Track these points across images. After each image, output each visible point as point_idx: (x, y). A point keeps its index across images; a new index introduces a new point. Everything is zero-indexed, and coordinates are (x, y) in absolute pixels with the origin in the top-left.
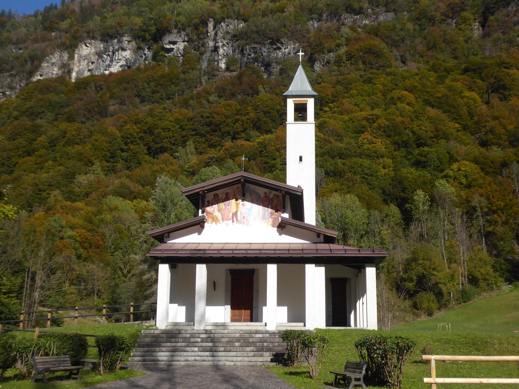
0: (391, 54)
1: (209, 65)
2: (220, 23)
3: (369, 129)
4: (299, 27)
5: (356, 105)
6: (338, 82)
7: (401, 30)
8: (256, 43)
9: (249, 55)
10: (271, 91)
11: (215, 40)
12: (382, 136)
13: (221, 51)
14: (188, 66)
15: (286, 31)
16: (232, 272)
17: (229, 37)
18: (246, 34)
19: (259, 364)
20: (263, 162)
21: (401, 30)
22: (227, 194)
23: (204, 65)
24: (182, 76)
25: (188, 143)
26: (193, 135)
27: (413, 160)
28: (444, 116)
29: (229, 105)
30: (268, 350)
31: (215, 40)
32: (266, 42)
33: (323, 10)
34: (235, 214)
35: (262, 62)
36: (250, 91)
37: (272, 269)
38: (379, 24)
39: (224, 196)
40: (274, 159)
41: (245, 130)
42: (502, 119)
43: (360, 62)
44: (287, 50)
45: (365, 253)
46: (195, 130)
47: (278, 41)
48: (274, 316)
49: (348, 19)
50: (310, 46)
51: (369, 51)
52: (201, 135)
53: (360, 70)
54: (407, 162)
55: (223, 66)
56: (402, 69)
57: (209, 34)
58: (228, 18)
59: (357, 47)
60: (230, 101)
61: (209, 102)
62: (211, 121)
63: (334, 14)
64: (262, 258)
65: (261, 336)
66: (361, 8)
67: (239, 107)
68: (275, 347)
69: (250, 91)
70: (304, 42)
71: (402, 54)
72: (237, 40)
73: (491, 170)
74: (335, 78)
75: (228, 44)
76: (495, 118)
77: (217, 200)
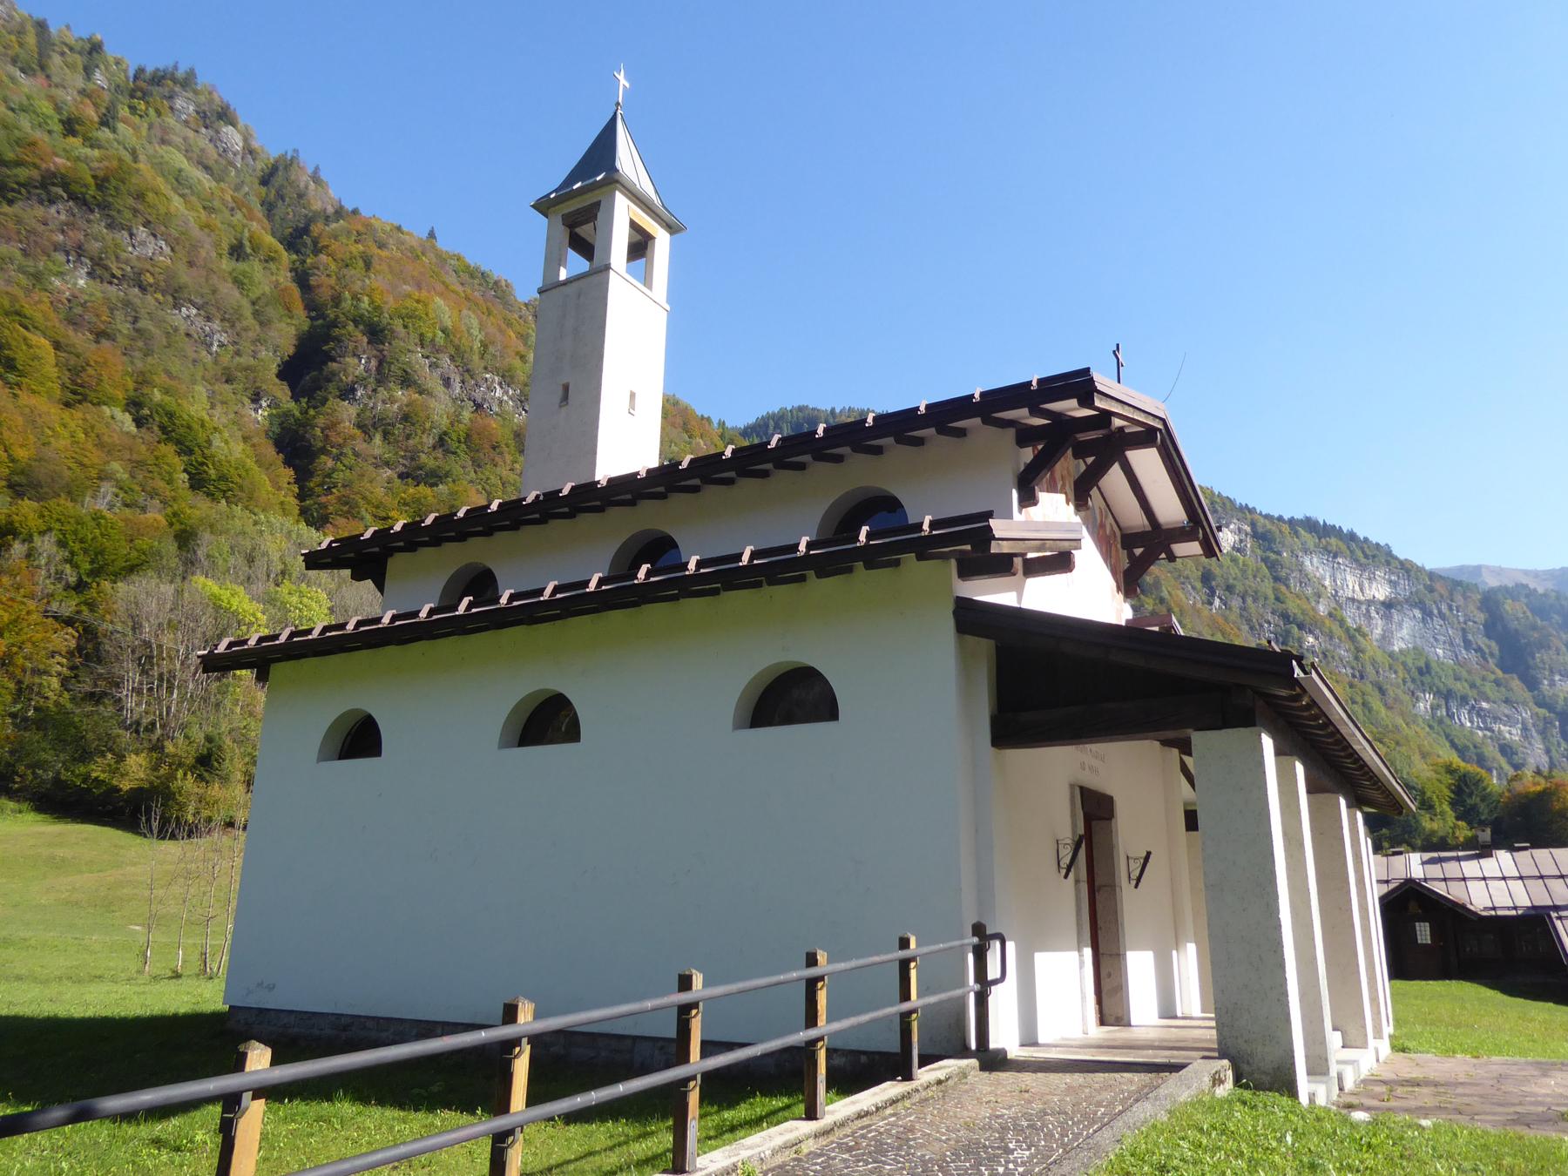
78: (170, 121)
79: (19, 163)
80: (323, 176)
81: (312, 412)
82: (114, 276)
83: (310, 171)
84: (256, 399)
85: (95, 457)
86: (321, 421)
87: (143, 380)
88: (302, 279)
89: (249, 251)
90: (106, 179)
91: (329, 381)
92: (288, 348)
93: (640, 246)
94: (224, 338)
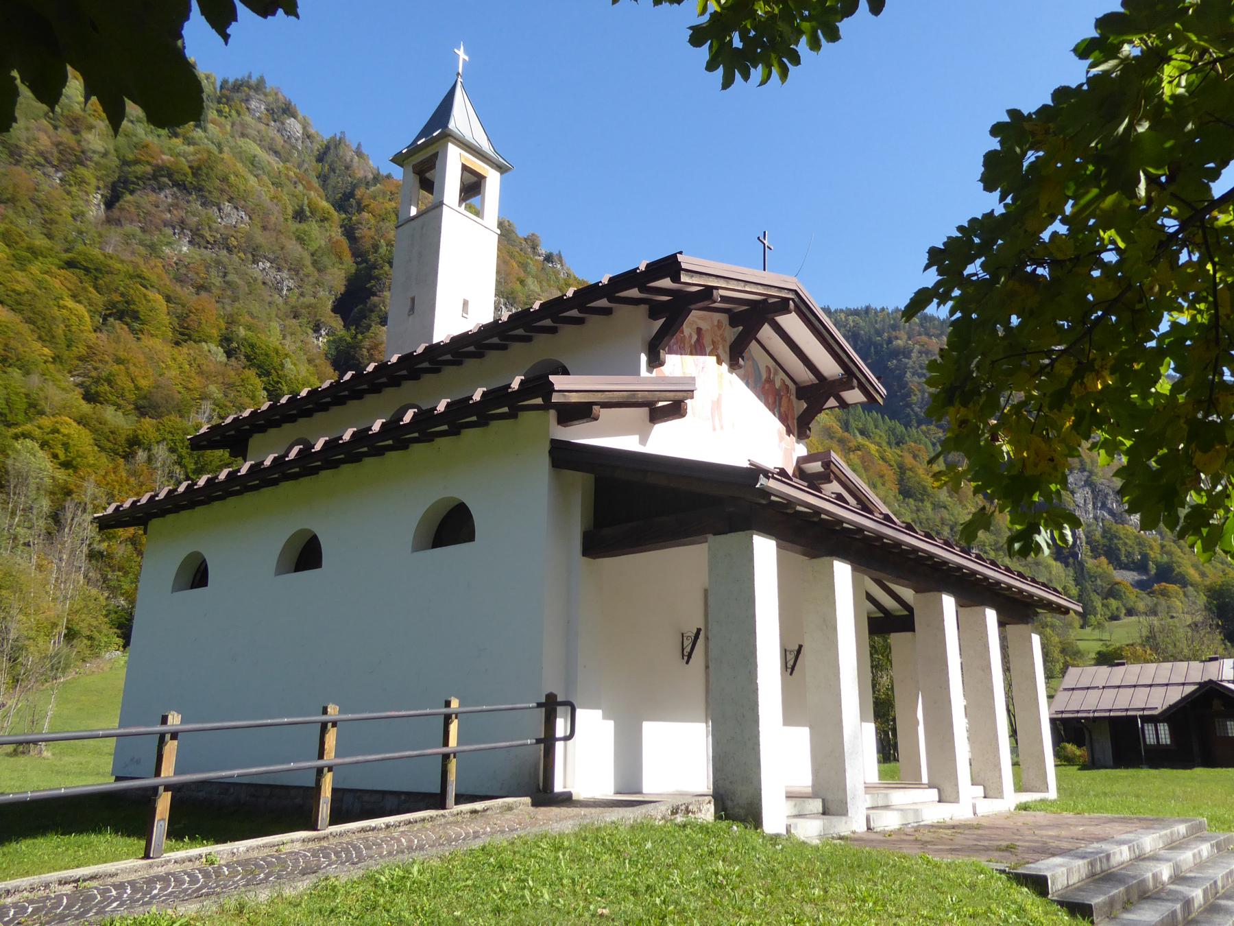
28: (25, 328)
42: (131, 365)
73: (109, 445)
76: (119, 361)
78: (248, 118)
79: (137, 162)
80: (364, 150)
81: (360, 337)
82: (208, 242)
83: (354, 147)
84: (317, 329)
85: (196, 382)
86: (367, 343)
87: (231, 321)
88: (350, 232)
89: (308, 214)
90: (199, 168)
91: (372, 311)
92: (340, 288)
93: (472, 187)
94: (291, 284)
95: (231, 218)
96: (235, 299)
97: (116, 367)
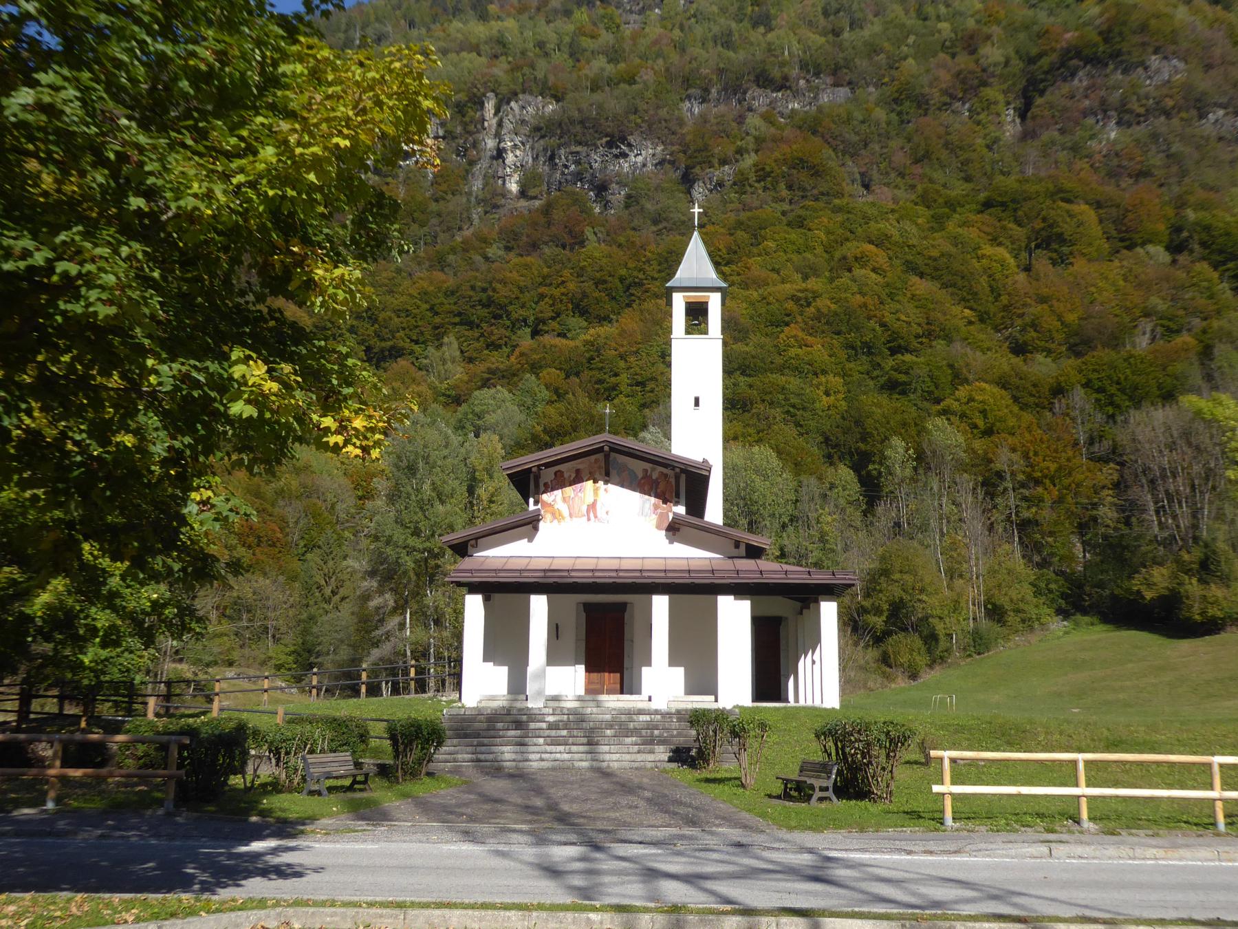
0: (843, 169)
1: (485, 185)
2: (508, 103)
3: (799, 319)
4: (663, 113)
5: (773, 270)
6: (740, 224)
7: (863, 122)
8: (580, 144)
9: (566, 167)
10: (608, 238)
11: (498, 135)
12: (823, 332)
13: (510, 158)
14: (444, 187)
15: (639, 121)
16: (588, 607)
17: (526, 130)
18: (560, 124)
19: (649, 765)
20: (594, 379)
21: (863, 122)
22: (578, 471)
23: (477, 185)
24: (433, 206)
25: (446, 340)
26: (455, 324)
27: (883, 380)
28: (942, 295)
29: (527, 266)
30: (663, 742)
31: (498, 135)
32: (599, 143)
33: (710, 81)
34: (592, 507)
35: (591, 182)
36: (567, 239)
37: (660, 605)
38: (820, 109)
39: (573, 475)
40: (616, 375)
41: (558, 315)
42: (1054, 302)
43: (782, 186)
44: (640, 159)
45: (820, 578)
46: (459, 314)
47: (623, 139)
48: (662, 685)
49: (760, 99)
50: (685, 152)
51: (800, 163)
52: (471, 325)
53: (783, 200)
54: (871, 383)
55: (513, 187)
56: (862, 200)
57: (486, 124)
58: (524, 92)
59: (777, 154)
60: (529, 259)
61: (487, 259)
62: (489, 298)
63: (734, 88)
64: (645, 585)
65: (647, 718)
66: (786, 78)
67: (546, 270)
68: (672, 736)
69: (567, 239)
70: (672, 144)
71: (863, 170)
72: (542, 137)
73: (1032, 400)
74: (732, 217)
75: (523, 144)
76: (1043, 300)
77: (560, 482)
79: (1040, 56)
82: (1139, 115)
90: (1110, 30)
95: (1164, 72)
96: (1183, 174)
97: (1040, 307)
